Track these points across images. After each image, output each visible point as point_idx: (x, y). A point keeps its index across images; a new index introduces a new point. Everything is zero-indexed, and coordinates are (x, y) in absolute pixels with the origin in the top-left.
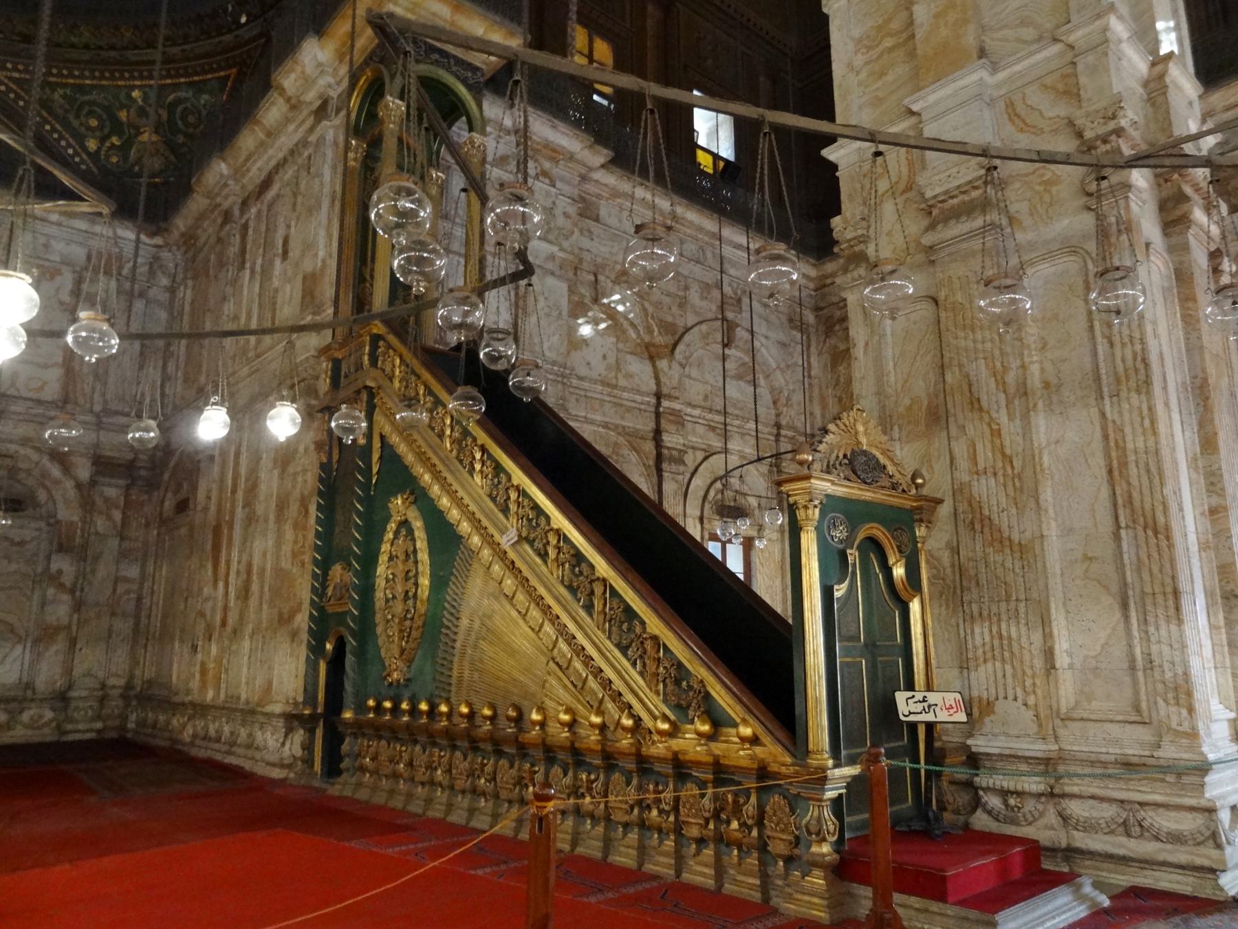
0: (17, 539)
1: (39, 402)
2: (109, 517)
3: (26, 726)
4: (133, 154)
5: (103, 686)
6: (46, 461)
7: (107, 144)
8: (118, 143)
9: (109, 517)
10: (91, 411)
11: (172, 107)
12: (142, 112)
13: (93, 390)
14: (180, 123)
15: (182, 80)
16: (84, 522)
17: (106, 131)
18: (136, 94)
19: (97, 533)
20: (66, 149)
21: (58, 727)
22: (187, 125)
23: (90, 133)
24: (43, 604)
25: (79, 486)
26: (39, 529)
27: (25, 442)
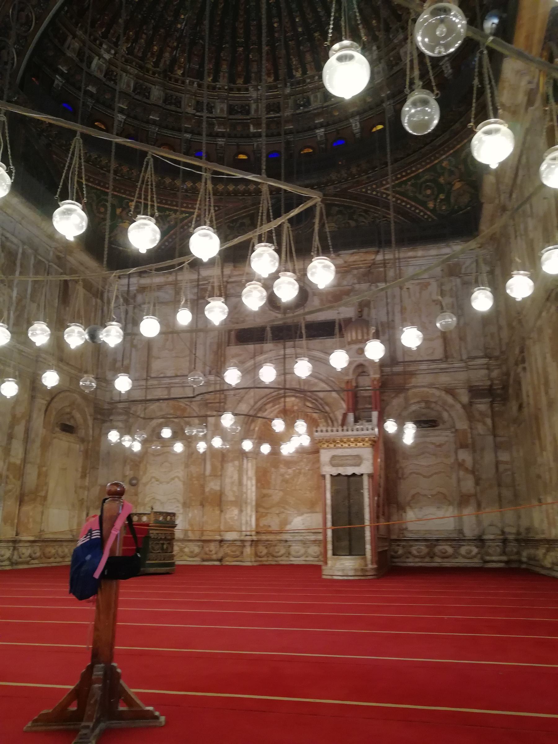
0: (438, 444)
1: (433, 361)
2: (484, 424)
3: (464, 557)
4: (452, 200)
5: (503, 533)
6: (443, 394)
8: (443, 197)
9: (484, 424)
10: (462, 360)
13: (460, 347)
16: (471, 428)
18: (445, 164)
19: (479, 435)
20: (419, 213)
21: (482, 558)
24: (459, 481)
25: (464, 406)
26: (447, 436)
27: (431, 386)
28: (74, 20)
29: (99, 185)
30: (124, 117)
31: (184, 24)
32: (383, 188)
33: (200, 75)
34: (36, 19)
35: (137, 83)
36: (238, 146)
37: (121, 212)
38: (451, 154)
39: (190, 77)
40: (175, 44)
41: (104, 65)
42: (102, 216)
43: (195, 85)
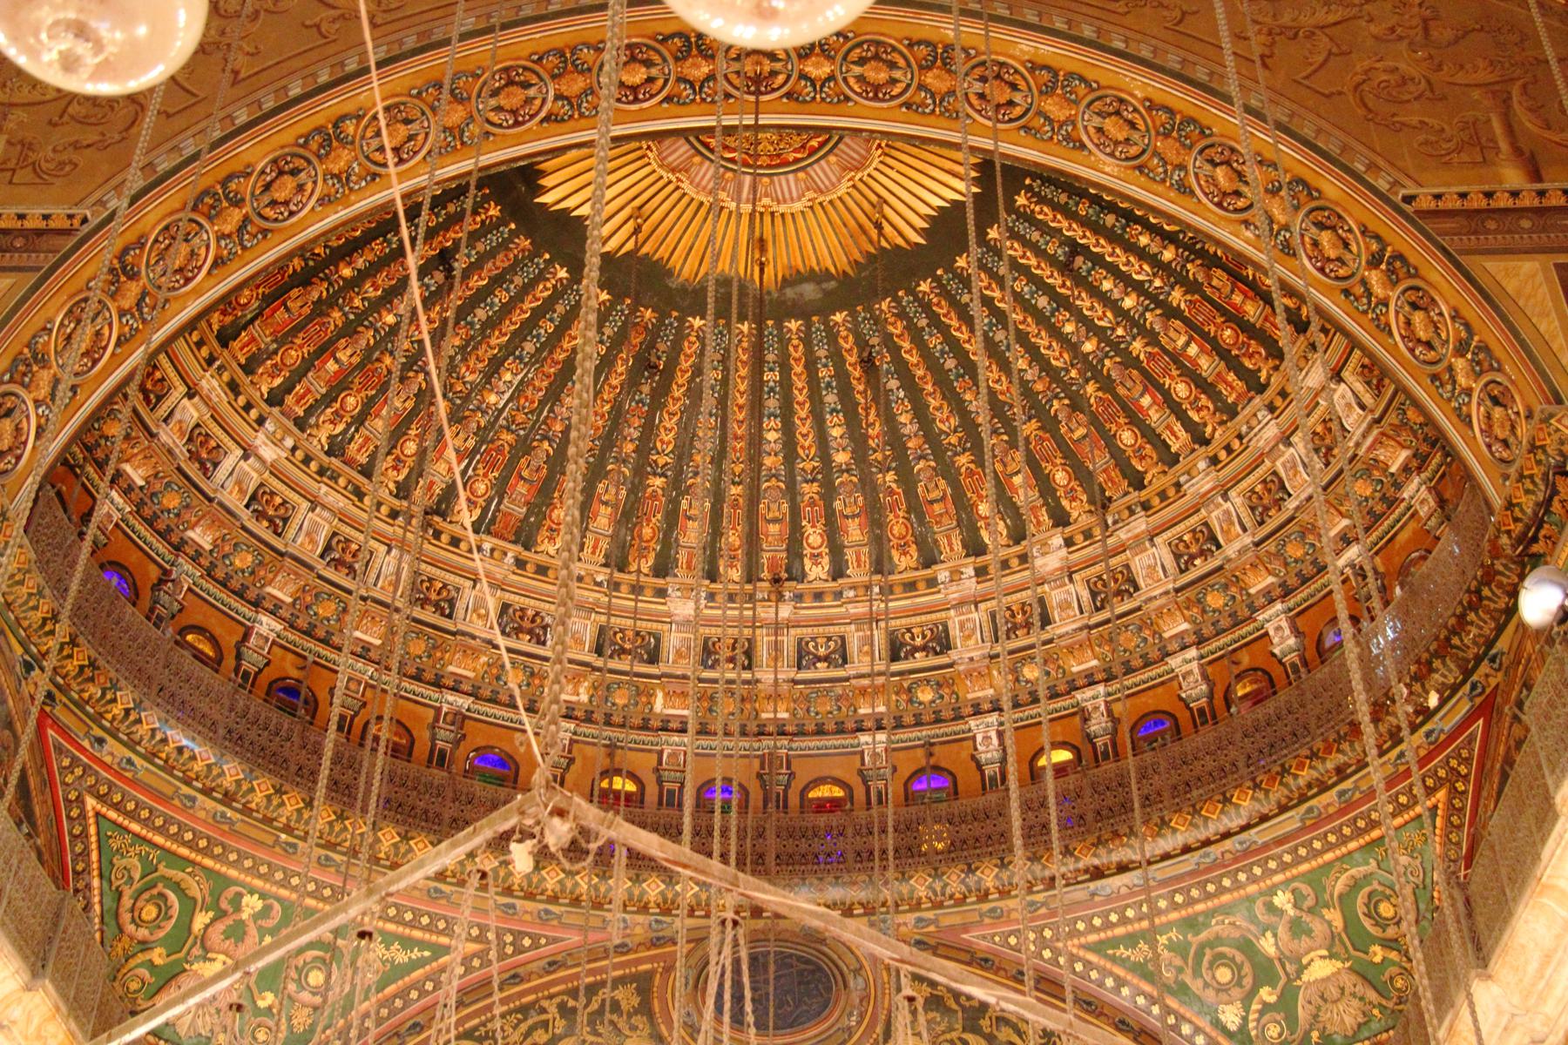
7: (1255, 1006)
8: (1272, 999)
11: (1345, 900)
12: (1297, 929)
14: (1367, 923)
15: (1353, 845)
17: (1248, 982)
22: (1381, 923)
23: (1224, 996)
28: (205, 352)
29: (161, 830)
30: (279, 627)
31: (507, 396)
32: (1076, 941)
33: (525, 536)
34: (118, 344)
35: (335, 534)
36: (612, 748)
37: (207, 927)
38: (1303, 875)
39: (496, 536)
40: (471, 443)
41: (255, 475)
42: (143, 933)
43: (509, 559)
